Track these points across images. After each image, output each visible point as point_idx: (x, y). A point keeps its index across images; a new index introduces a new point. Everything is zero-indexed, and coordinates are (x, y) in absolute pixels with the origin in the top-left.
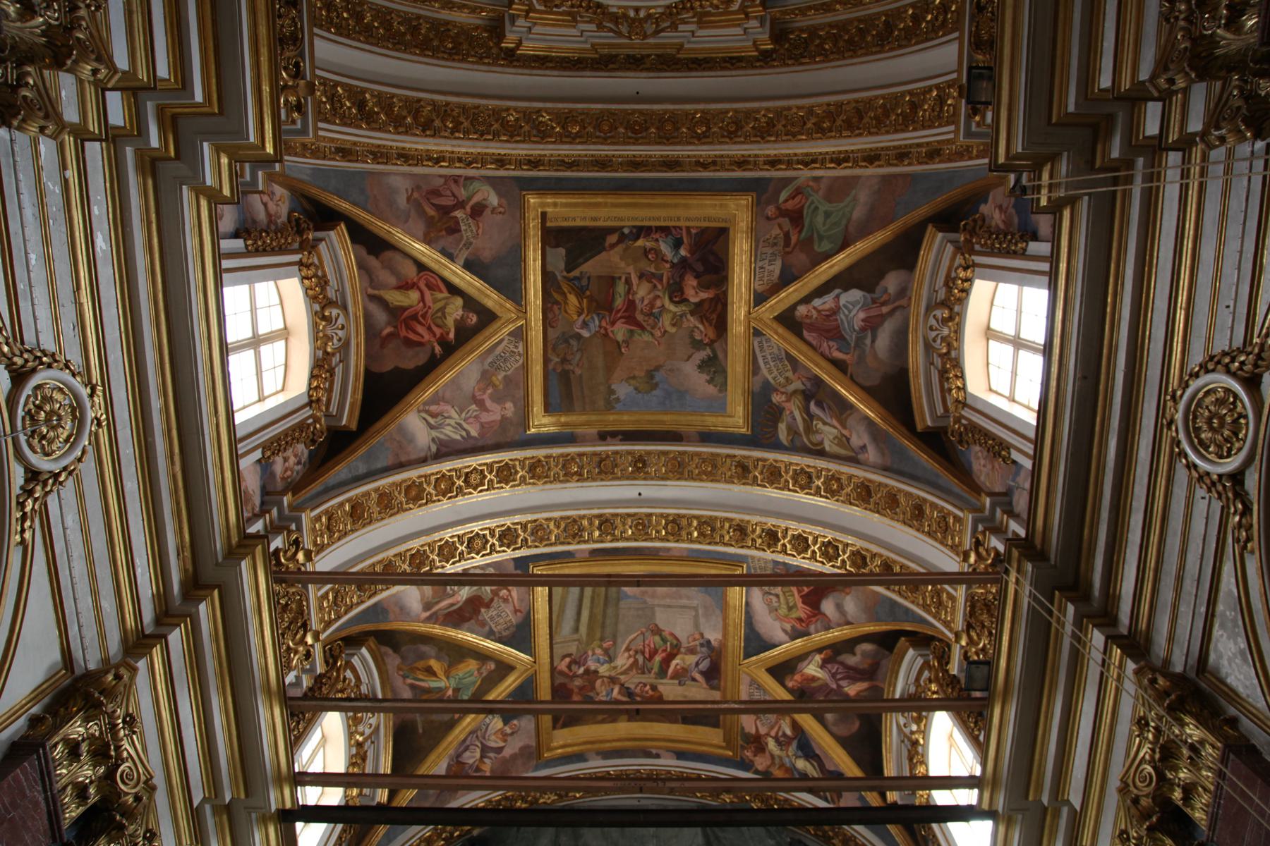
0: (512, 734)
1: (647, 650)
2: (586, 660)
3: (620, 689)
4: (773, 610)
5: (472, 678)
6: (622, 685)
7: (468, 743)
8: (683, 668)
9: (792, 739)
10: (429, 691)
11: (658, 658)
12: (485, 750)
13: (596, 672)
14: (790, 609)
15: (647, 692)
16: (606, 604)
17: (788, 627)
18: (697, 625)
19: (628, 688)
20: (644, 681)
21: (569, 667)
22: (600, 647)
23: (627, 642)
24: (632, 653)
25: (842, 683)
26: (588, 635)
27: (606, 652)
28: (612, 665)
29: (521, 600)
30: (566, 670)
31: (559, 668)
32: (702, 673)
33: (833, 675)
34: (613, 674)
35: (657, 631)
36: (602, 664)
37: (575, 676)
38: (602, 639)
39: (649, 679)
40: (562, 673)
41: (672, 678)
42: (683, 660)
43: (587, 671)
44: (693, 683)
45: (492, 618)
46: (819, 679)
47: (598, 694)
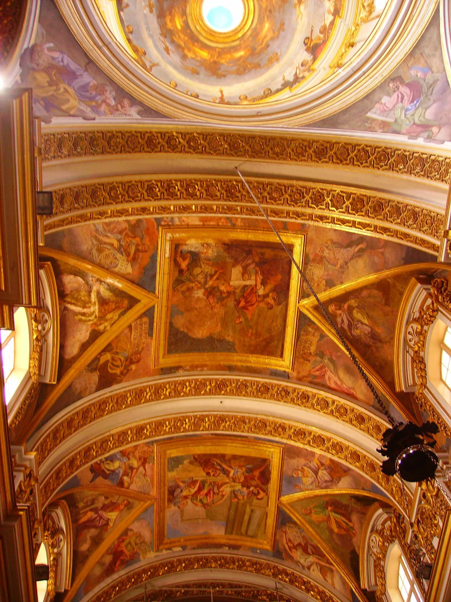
0: (298, 470)
1: (211, 495)
2: (248, 494)
3: (229, 474)
4: (139, 536)
5: (315, 510)
6: (228, 476)
7: (324, 485)
8: (190, 487)
9: (123, 475)
10: (342, 514)
11: (205, 491)
12: (316, 473)
13: (243, 486)
14: (130, 543)
15: (213, 471)
16: (234, 520)
17: (130, 533)
18: (182, 512)
19: (225, 474)
20: (214, 478)
21: (259, 493)
22: (239, 499)
23: (223, 500)
24: (221, 493)
25: (95, 516)
26: (245, 507)
27: (236, 496)
28: (233, 489)
29: (282, 536)
30: (260, 491)
31: (264, 494)
32: (178, 486)
33: (101, 517)
34: (233, 484)
35: (204, 505)
36: (239, 490)
37: (256, 487)
38: (238, 503)
39: (211, 479)
40: (264, 491)
41: (197, 481)
42: (190, 491)
43: (248, 487)
44: (184, 480)
45: (299, 537)
46: (110, 511)
47: (243, 473)
